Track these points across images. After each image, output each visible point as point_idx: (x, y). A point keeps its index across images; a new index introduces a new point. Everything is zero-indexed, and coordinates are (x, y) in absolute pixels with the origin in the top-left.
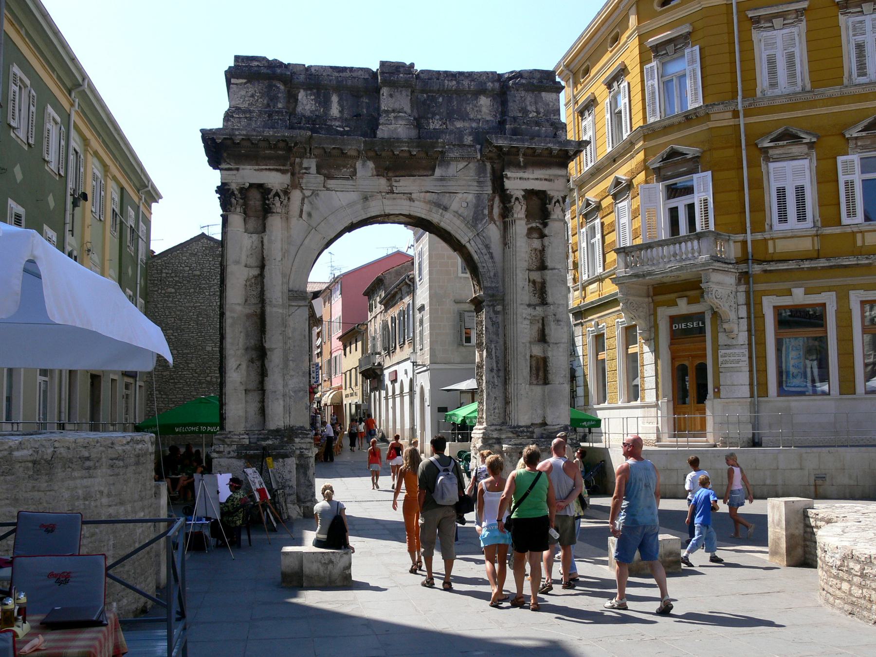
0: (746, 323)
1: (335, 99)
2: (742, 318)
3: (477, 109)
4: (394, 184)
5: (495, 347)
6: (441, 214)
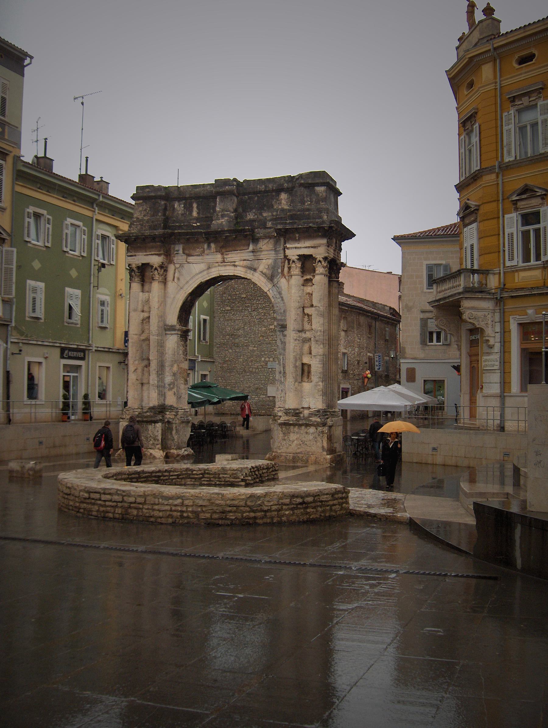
0: (499, 336)
1: (195, 205)
2: (497, 332)
3: (279, 202)
4: (225, 257)
5: (283, 358)
6: (253, 274)
